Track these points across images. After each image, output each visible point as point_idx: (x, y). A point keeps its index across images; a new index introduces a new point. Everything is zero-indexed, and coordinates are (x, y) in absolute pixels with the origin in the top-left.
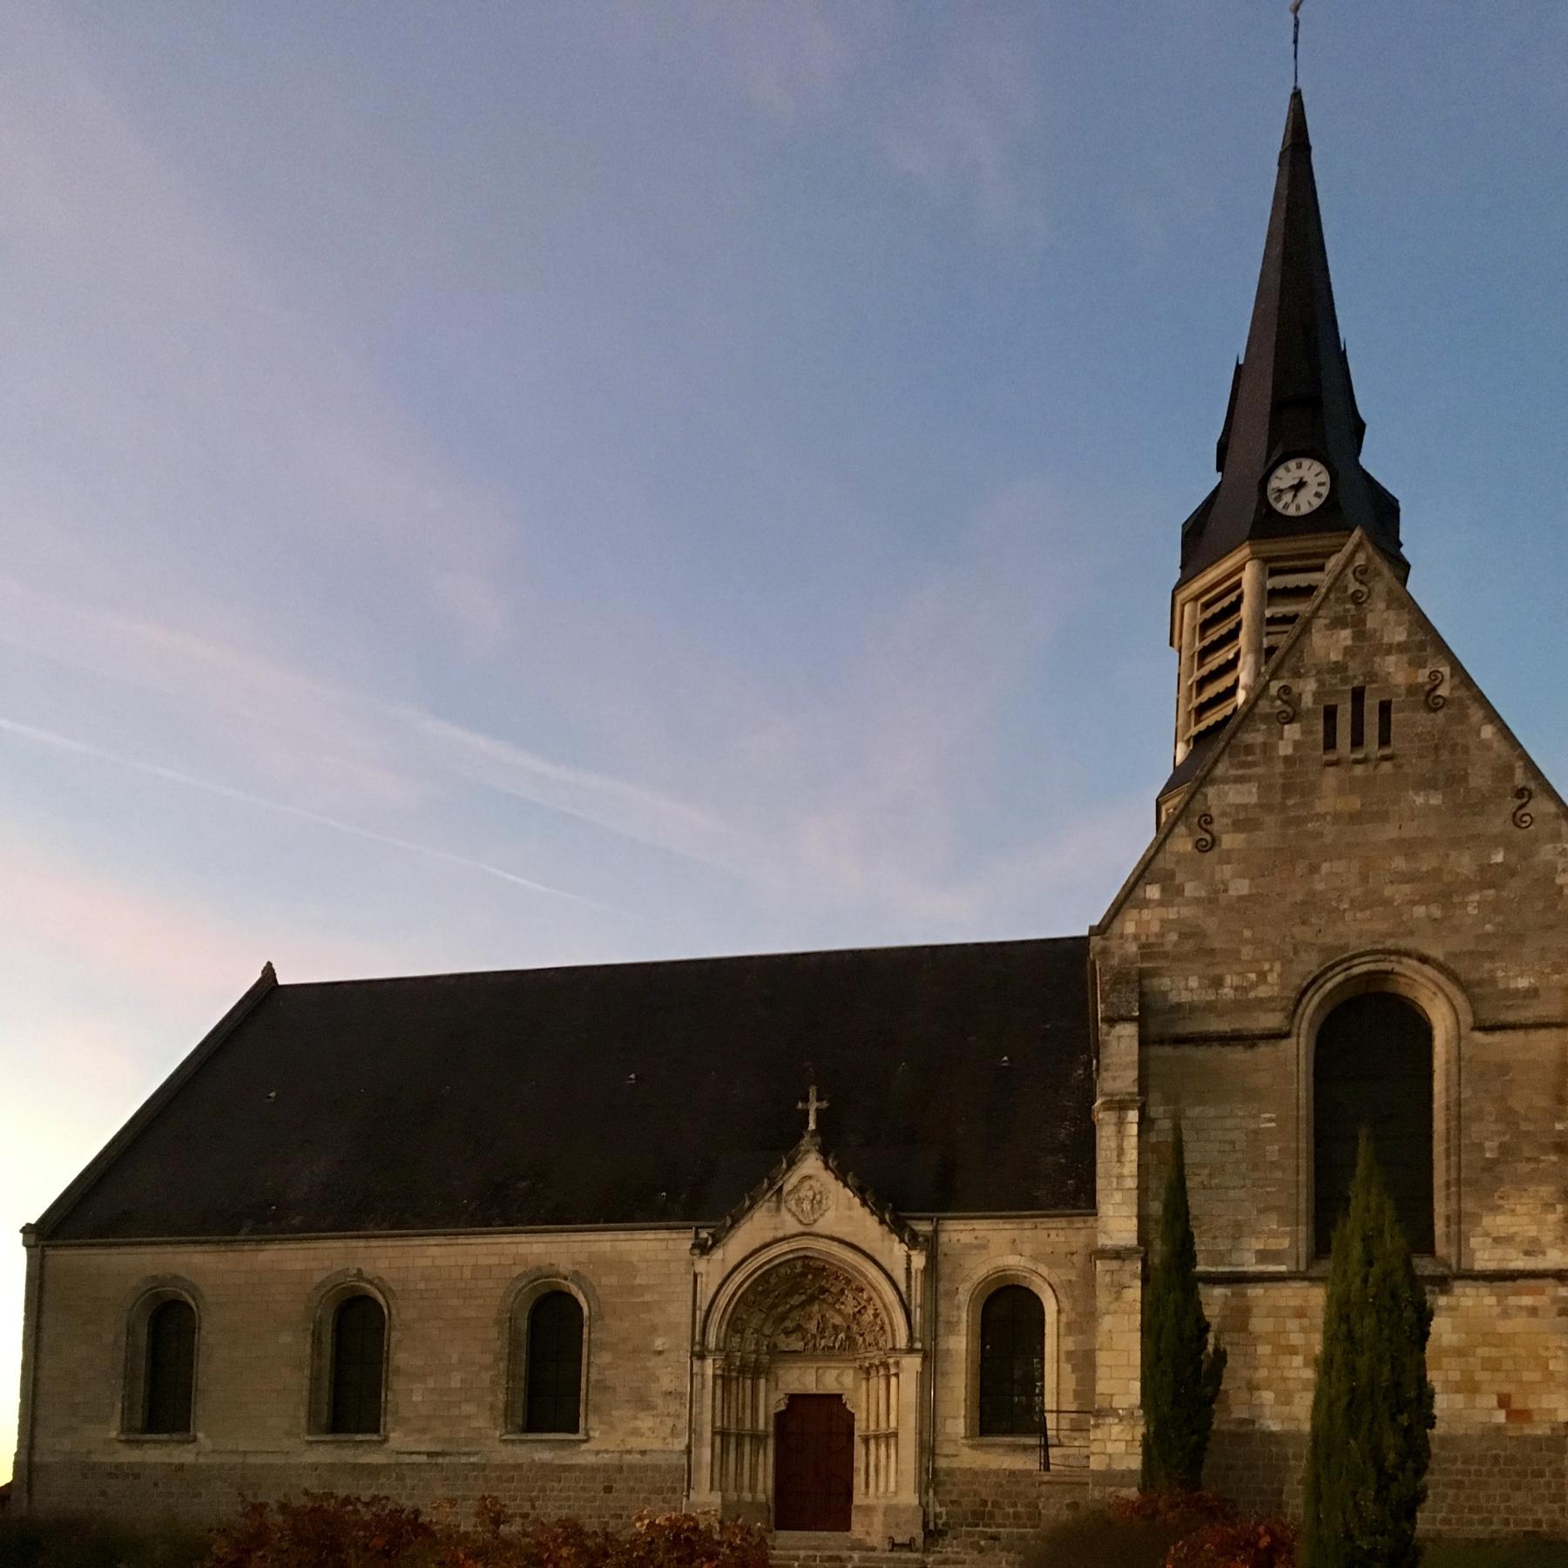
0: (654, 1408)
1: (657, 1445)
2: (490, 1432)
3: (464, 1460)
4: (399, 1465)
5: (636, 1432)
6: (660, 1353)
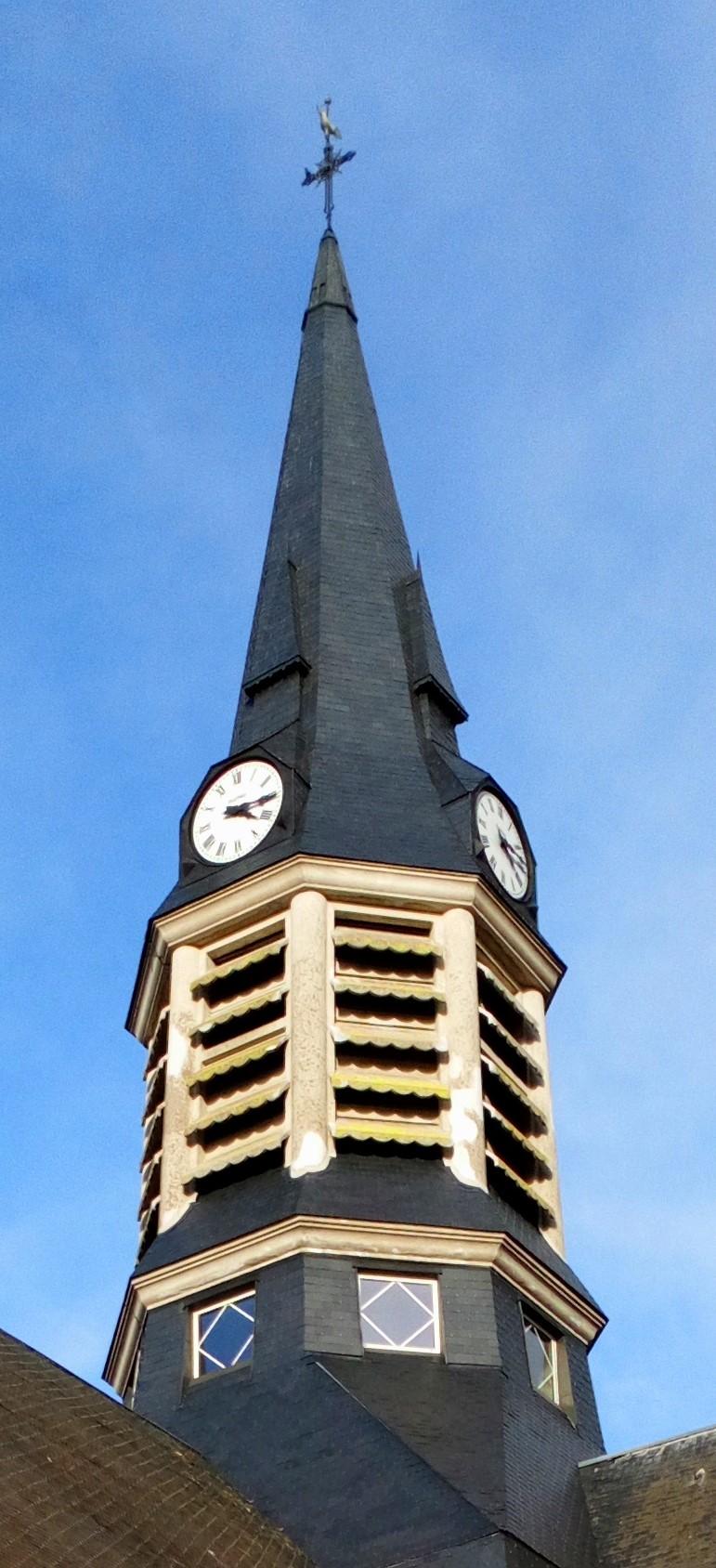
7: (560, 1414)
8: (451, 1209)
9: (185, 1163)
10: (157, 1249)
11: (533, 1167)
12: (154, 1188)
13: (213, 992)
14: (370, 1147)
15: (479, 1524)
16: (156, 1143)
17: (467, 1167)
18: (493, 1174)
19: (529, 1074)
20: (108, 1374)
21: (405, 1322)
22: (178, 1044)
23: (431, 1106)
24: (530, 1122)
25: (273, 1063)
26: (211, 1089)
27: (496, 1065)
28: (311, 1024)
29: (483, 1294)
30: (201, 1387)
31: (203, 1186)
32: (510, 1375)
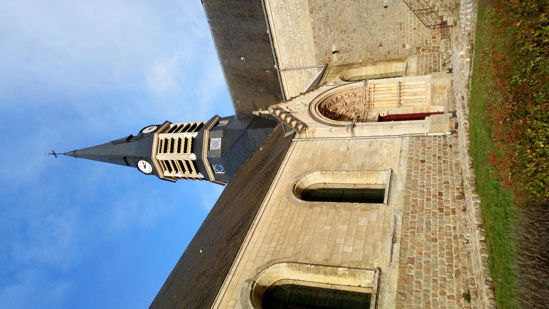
0: (377, 150)
1: (398, 149)
2: (381, 212)
3: (399, 223)
4: (400, 262)
5: (390, 155)
6: (348, 149)
7: (229, 122)
8: (201, 136)
9: (194, 174)
10: (206, 178)
11: (195, 125)
12: (198, 179)
13: (170, 170)
14: (192, 148)
15: (245, 133)
16: (191, 178)
17: (195, 135)
18: (196, 131)
19: (182, 126)
20: (224, 185)
21: (217, 143)
22: (177, 175)
23: (186, 140)
24: (188, 126)
25: (180, 162)
26: (184, 171)
27: (181, 130)
28: (175, 156)
29: (213, 132)
30: (226, 172)
31: (198, 172)
32: (224, 128)
